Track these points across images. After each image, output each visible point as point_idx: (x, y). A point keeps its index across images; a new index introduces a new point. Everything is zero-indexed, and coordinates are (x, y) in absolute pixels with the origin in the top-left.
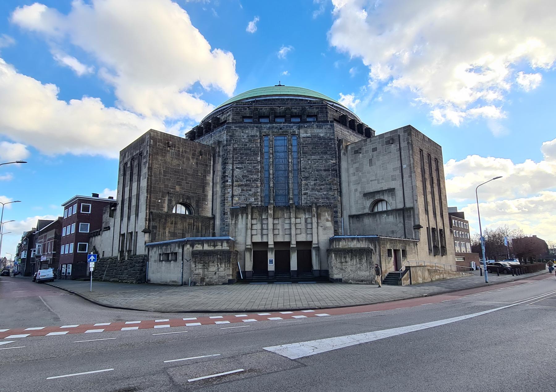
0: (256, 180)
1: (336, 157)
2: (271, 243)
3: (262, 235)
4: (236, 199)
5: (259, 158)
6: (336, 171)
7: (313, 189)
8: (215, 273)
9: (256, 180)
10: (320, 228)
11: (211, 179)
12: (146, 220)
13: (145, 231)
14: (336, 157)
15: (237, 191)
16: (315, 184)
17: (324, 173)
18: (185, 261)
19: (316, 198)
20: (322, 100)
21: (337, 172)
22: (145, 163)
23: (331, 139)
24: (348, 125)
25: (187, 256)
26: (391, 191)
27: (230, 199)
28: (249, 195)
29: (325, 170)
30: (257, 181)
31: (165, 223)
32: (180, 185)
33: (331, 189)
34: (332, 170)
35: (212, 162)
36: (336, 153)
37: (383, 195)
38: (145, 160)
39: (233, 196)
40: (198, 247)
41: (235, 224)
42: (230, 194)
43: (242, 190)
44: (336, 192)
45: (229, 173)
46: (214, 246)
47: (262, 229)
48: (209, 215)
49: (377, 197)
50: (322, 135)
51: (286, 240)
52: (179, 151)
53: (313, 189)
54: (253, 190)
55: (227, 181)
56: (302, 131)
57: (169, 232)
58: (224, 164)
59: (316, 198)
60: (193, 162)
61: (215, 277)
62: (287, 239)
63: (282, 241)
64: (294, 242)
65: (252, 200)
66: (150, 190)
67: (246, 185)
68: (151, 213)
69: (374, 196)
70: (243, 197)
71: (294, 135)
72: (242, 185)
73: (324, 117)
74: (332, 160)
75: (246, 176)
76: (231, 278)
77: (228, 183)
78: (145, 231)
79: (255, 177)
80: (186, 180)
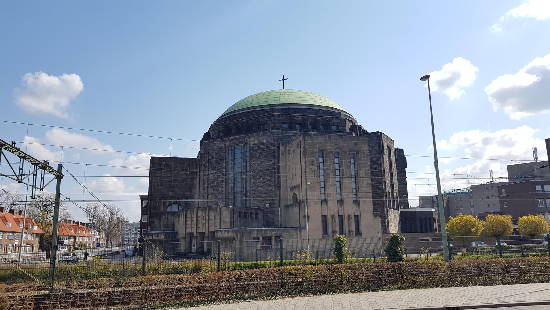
0: (222, 182)
1: (275, 158)
3: (192, 227)
4: (210, 197)
6: (275, 169)
7: (258, 186)
9: (222, 182)
10: (222, 223)
11: (198, 183)
14: (275, 158)
16: (259, 182)
17: (266, 173)
23: (271, 144)
28: (218, 194)
29: (266, 170)
31: (160, 219)
32: (173, 191)
33: (270, 185)
34: (272, 170)
35: (198, 171)
36: (274, 155)
41: (178, 221)
46: (158, 236)
50: (265, 141)
52: (171, 167)
54: (220, 189)
56: (252, 139)
57: (163, 225)
60: (182, 173)
64: (207, 233)
67: (216, 186)
70: (214, 196)
72: (213, 186)
73: (271, 123)
79: (222, 179)
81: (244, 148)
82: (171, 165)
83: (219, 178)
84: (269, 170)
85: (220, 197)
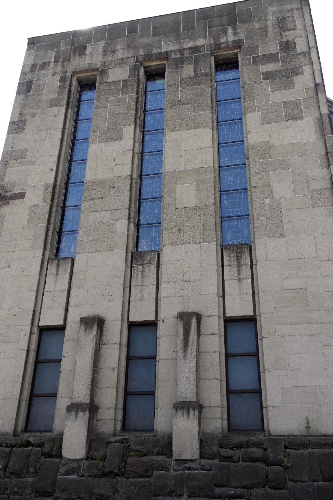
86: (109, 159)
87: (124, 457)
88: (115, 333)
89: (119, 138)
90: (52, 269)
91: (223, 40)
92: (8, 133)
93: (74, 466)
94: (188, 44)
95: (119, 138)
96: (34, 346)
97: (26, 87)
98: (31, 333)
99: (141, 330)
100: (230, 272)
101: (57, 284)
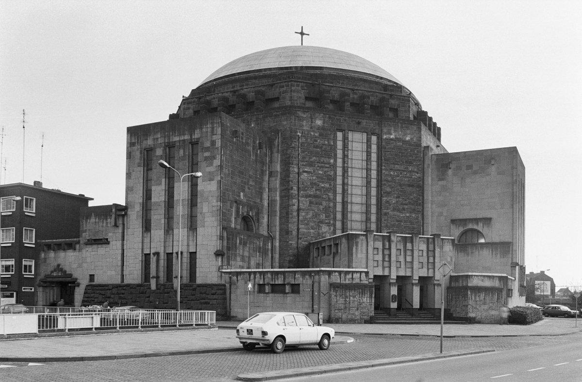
2: (394, 276)
3: (384, 268)
4: (303, 214)
5: (332, 161)
8: (358, 309)
9: (328, 190)
12: (220, 239)
13: (218, 254)
15: (304, 203)
18: (322, 294)
19: (398, 221)
20: (399, 87)
21: (420, 187)
22: (210, 160)
24: (432, 130)
25: (324, 288)
26: (487, 221)
27: (295, 214)
29: (409, 186)
30: (329, 192)
32: (244, 191)
37: (477, 224)
38: (207, 154)
39: (298, 210)
40: (336, 279)
42: (295, 207)
43: (311, 203)
44: (420, 215)
45: (293, 176)
47: (384, 260)
48: (265, 233)
49: (470, 226)
51: (407, 275)
53: (394, 210)
54: (324, 203)
55: (292, 188)
58: (286, 164)
59: (398, 221)
61: (356, 313)
62: (409, 274)
63: (404, 275)
65: (323, 217)
66: (222, 198)
67: (315, 196)
68: (224, 228)
69: (465, 225)
71: (373, 134)
72: (310, 196)
74: (418, 173)
75: (315, 184)
76: (372, 314)
77: (292, 191)
78: (218, 254)
79: (327, 185)
80: (248, 184)
81: (369, 141)
82: (242, 139)
83: (323, 182)
84: (412, 186)
85: (323, 217)
86: (159, 194)
87: (164, 290)
88: (162, 256)
89: (160, 184)
90: (145, 235)
91: (193, 137)
92: (126, 179)
93: (154, 292)
94: (182, 138)
95: (160, 184)
96: (144, 259)
97: (129, 156)
98: (142, 256)
99: (169, 256)
100: (191, 238)
101: (147, 240)
